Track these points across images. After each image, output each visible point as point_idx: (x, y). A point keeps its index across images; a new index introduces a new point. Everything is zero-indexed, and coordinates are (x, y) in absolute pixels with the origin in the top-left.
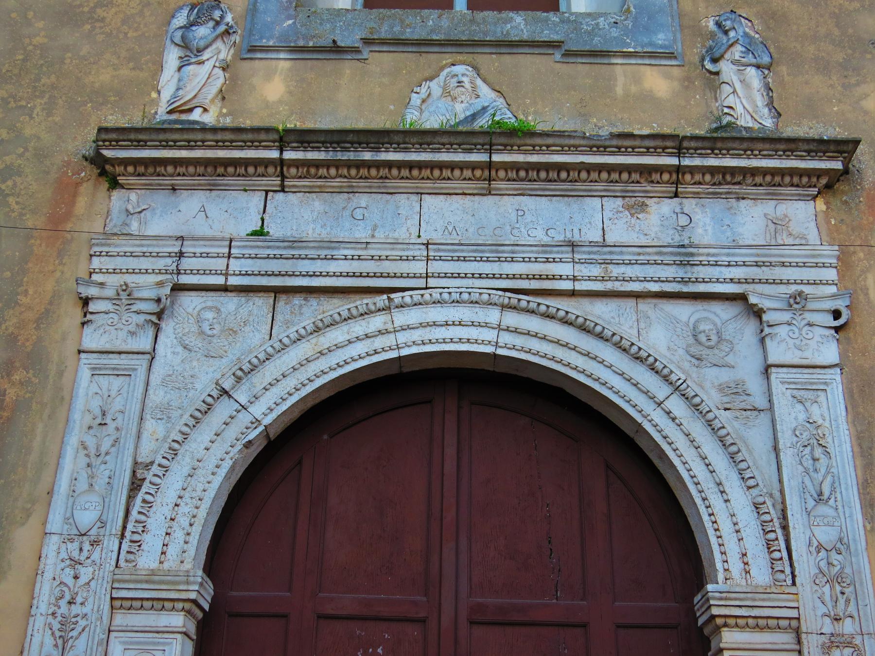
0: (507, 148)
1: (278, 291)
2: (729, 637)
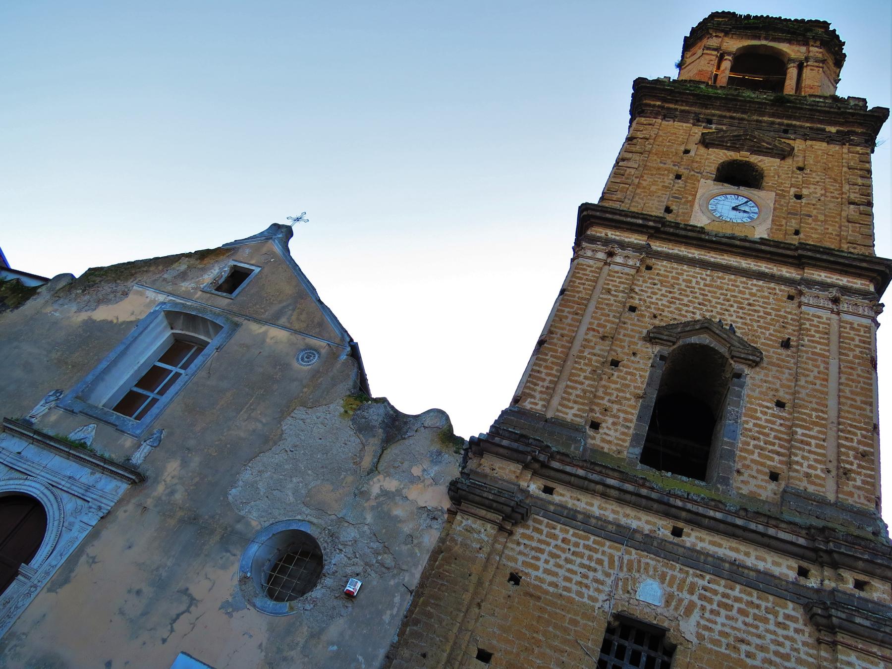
0: (74, 450)
1: (12, 468)
2: (20, 577)
